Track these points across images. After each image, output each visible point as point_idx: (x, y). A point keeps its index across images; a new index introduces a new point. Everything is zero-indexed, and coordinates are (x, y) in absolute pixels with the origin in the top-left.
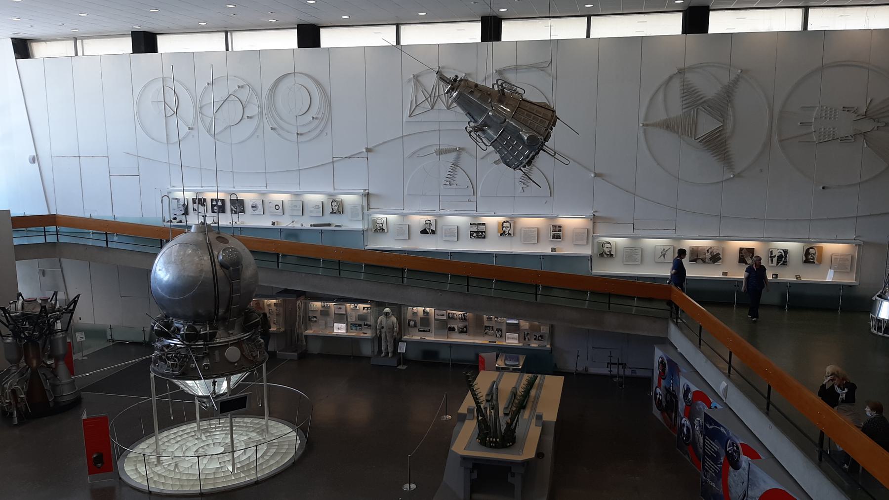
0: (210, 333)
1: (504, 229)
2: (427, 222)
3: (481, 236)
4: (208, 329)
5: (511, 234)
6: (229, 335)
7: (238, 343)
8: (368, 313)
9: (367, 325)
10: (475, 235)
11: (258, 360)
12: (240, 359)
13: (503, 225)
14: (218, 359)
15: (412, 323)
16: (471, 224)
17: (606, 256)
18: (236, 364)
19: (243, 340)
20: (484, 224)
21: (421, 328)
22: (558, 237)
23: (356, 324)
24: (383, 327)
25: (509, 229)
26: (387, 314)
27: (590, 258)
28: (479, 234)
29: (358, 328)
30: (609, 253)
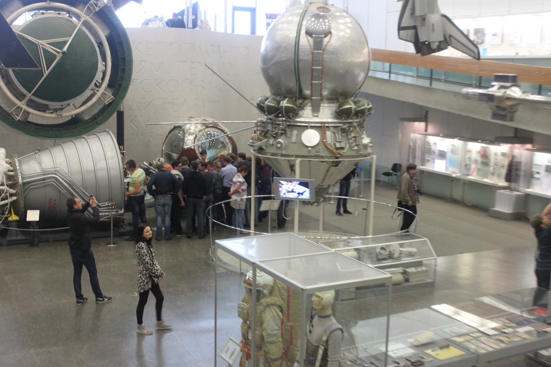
0: (286, 107)
7: (322, 128)
11: (341, 153)
12: (318, 144)
14: (294, 139)
18: (310, 148)
19: (328, 127)
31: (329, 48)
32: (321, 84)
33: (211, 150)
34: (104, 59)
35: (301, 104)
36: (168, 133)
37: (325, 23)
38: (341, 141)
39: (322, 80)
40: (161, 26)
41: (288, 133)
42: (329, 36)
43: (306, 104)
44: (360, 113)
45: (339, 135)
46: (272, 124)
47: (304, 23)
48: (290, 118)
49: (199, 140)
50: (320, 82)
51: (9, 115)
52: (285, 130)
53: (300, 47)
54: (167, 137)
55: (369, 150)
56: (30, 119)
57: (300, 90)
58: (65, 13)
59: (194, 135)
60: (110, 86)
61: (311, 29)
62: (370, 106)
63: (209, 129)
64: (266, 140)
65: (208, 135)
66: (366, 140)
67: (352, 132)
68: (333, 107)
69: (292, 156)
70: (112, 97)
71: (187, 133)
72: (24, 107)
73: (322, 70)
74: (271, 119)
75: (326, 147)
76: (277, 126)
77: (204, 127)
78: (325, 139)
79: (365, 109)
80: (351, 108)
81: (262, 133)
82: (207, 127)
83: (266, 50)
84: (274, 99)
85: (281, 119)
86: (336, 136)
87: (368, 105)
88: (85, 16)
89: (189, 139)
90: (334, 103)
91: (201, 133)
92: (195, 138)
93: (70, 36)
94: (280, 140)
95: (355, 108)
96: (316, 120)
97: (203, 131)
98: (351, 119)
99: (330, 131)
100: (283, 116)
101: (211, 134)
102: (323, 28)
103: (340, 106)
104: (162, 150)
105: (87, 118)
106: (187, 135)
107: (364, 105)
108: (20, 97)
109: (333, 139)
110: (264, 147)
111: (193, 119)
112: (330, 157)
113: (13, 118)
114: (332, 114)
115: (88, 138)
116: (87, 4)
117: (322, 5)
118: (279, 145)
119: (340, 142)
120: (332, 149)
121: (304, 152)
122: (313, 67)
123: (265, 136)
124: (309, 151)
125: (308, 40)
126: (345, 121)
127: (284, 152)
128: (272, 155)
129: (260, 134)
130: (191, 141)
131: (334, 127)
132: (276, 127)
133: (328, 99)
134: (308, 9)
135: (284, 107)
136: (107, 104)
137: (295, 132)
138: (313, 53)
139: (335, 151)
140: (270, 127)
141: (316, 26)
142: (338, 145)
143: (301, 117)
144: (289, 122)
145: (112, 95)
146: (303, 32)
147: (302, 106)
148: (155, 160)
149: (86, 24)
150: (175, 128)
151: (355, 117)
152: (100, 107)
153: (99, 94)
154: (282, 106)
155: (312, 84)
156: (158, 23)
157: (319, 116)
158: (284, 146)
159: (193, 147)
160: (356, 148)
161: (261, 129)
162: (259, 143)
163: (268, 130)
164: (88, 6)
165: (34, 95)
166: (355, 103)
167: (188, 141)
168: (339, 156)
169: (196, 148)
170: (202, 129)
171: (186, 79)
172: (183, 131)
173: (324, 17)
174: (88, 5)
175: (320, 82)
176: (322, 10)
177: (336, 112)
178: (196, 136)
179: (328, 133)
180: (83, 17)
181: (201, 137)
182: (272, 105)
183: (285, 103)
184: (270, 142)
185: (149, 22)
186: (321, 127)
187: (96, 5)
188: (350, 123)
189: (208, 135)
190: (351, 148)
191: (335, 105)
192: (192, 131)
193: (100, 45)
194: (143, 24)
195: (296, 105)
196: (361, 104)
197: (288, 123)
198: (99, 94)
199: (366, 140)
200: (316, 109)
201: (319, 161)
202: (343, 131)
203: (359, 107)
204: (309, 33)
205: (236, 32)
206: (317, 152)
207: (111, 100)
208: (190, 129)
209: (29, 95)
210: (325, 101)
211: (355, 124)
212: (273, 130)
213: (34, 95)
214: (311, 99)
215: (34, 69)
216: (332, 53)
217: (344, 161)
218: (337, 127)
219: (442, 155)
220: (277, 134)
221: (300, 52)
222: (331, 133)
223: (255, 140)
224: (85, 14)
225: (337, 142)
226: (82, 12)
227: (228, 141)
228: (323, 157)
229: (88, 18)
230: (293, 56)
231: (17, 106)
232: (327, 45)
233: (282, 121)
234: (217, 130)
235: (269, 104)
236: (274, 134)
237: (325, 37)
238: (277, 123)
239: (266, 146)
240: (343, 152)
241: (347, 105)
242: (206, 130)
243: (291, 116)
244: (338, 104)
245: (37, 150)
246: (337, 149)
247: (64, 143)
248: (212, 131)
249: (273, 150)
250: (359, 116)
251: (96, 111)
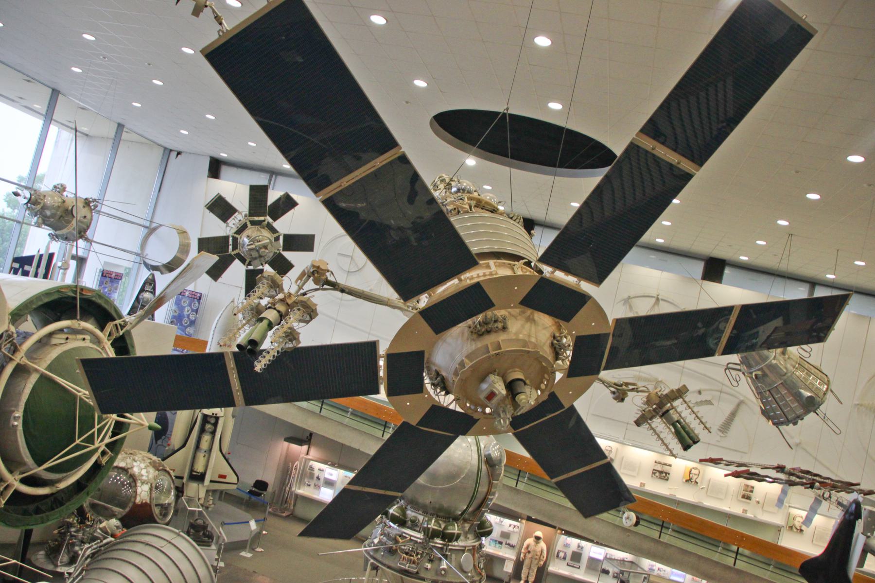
1: (691, 475)
2: (609, 449)
3: (664, 477)
4: (456, 529)
5: (697, 483)
8: (514, 532)
9: (509, 544)
10: (657, 474)
13: (691, 471)
15: (562, 555)
16: (656, 462)
17: (795, 530)
20: (670, 466)
21: (571, 563)
22: (749, 498)
23: (496, 541)
24: (529, 552)
25: (696, 476)
26: (538, 538)
27: (778, 529)
28: (662, 474)
29: (498, 545)
30: (799, 528)
59: (149, 484)
70: (110, 453)
71: (139, 481)
92: (151, 490)
106: (139, 484)
130: (146, 493)
135: (456, 534)
159: (148, 502)
178: (151, 485)
192: (144, 478)
208: (142, 476)
219: (329, 483)
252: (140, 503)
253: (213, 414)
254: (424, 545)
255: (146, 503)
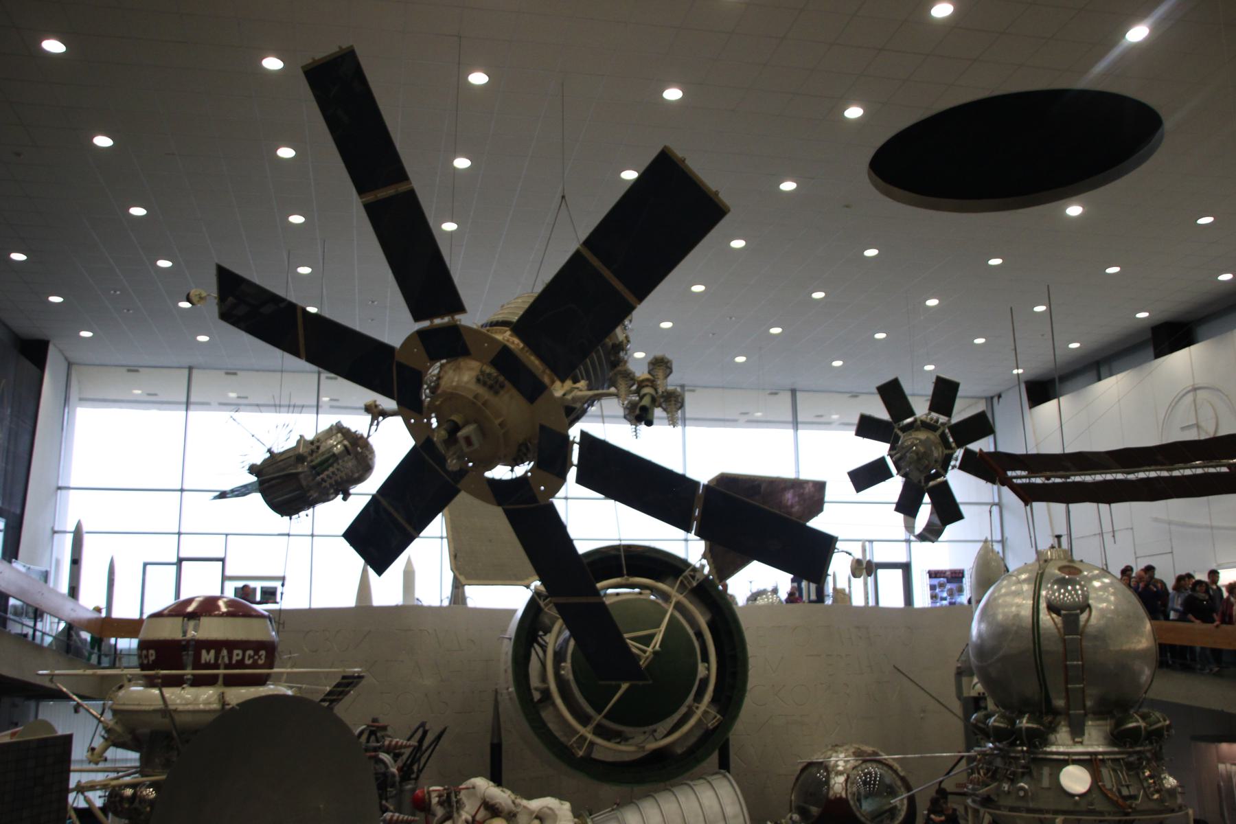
0: (1028, 729)
4: (1025, 721)
6: (1075, 743)
7: (1090, 762)
12: (1089, 790)
14: (1046, 782)
19: (1103, 761)
31: (1089, 630)
32: (1083, 690)
33: (869, 800)
34: (705, 658)
35: (1051, 723)
36: (799, 772)
37: (1076, 591)
38: (1131, 785)
39: (1085, 683)
40: (772, 598)
41: (1035, 774)
42: (1087, 610)
43: (1059, 724)
44: (1155, 736)
45: (1124, 772)
46: (1003, 757)
47: (1044, 593)
48: (1036, 747)
49: (852, 783)
50: (1082, 686)
51: (566, 747)
52: (1027, 768)
53: (1041, 632)
54: (797, 779)
55: (1180, 800)
56: (597, 755)
57: (1048, 700)
58: (648, 592)
59: (845, 775)
60: (714, 700)
61: (1055, 601)
62: (1168, 722)
63: (869, 765)
64: (996, 784)
65: (865, 775)
66: (1171, 782)
67: (1145, 768)
68: (1107, 725)
69: (1048, 812)
70: (719, 716)
71: (833, 773)
72: (590, 736)
73: (1083, 665)
74: (1000, 749)
75: (1106, 796)
76: (1012, 761)
77: (860, 762)
78: (1100, 781)
79: (1162, 728)
80: (1138, 729)
81: (987, 773)
82: (865, 761)
83: (980, 635)
84: (1002, 716)
85: (1020, 748)
86: (1119, 776)
87: (1165, 720)
88: (677, 594)
89: (837, 781)
90: (1106, 719)
91: (855, 772)
92: (846, 781)
93: (658, 626)
94: (1022, 784)
95: (1145, 728)
96: (1079, 749)
97: (859, 768)
98: (1141, 745)
99: (1106, 767)
100: (1022, 744)
101: (870, 773)
102: (1074, 599)
103: (1119, 723)
104: (791, 801)
105: (679, 751)
106: (832, 775)
107: (1159, 721)
108: (584, 719)
109: (1114, 780)
110: (994, 797)
111: (840, 749)
112: (1115, 814)
113: (573, 754)
114: (1105, 738)
115: (694, 785)
116: (679, 576)
117: (1065, 563)
118: (1022, 794)
119: (1128, 786)
120: (1115, 799)
121: (1066, 805)
122: (1068, 663)
123: (994, 778)
124: (1076, 803)
125: (1053, 619)
126: (1131, 750)
127: (1031, 805)
128: (1009, 811)
129: (985, 774)
130: (840, 785)
131: (1113, 760)
132: (1010, 763)
133: (1094, 713)
134: (1044, 571)
135: (1024, 728)
136: (711, 727)
137: (1046, 771)
138: (1064, 640)
139: (1120, 801)
140: (998, 762)
141: (1057, 594)
142: (1125, 792)
143: (1053, 744)
144: (1033, 753)
145: (718, 713)
146: (1043, 605)
147: (1053, 725)
148: (784, 819)
149: (679, 607)
150: (810, 764)
151: (1147, 742)
152: (698, 733)
153: (699, 713)
154: (1021, 728)
155: (1067, 690)
156: (770, 597)
157: (1086, 742)
158: (1030, 794)
159: (844, 795)
160: (1156, 796)
161: (985, 766)
162: (983, 791)
163: (997, 768)
164: (682, 582)
165: (605, 717)
166: (1144, 717)
167: (836, 785)
168: (1130, 810)
169: (849, 797)
170: (857, 764)
171: (822, 684)
172: (827, 769)
173: (1073, 582)
174: (680, 578)
175: (1082, 686)
176: (1067, 570)
177: (1112, 734)
178: (848, 777)
179: (1105, 772)
180: (675, 596)
181: (855, 778)
182: (1002, 725)
183: (1024, 723)
184: (1004, 788)
185: (758, 596)
186: (1090, 760)
187: (693, 577)
188: (1139, 752)
189: (865, 775)
190: (1147, 796)
191: (1108, 721)
192: (840, 768)
193: (699, 635)
194: (748, 600)
195: (1041, 724)
196: (1153, 718)
197: (1032, 756)
198: (699, 713)
199: (1171, 782)
200: (1077, 731)
201: (1095, 821)
202: (1130, 766)
203: (1151, 725)
204: (1052, 608)
205: (882, 604)
206: (1092, 804)
207: (716, 721)
209: (598, 718)
210: (1090, 716)
211: (1149, 755)
212: (1007, 767)
213: (605, 717)
214: (1068, 715)
215: (641, 683)
216: (1095, 638)
217: (1139, 820)
218: (1118, 760)
220: (1014, 773)
221: (1042, 639)
222: (1109, 771)
223: (979, 784)
224: (677, 591)
225: (1122, 786)
226: (672, 587)
227: (899, 783)
228: (1101, 813)
229: (681, 598)
230: (1031, 645)
231: (580, 734)
232: (1085, 625)
233: (1022, 751)
234: (880, 766)
235: (996, 724)
236: (1010, 774)
237: (1082, 612)
238: (1013, 755)
239: (998, 795)
240: (1136, 805)
241: (1132, 722)
242: (864, 766)
243: (1037, 743)
244: (1113, 722)
245: (615, 804)
246: (1125, 798)
247: (656, 791)
248: (872, 768)
249: (1010, 802)
250: (1154, 741)
251: (693, 740)
252: (833, 798)
253: (979, 694)
254: (1004, 755)
255: (841, 798)
